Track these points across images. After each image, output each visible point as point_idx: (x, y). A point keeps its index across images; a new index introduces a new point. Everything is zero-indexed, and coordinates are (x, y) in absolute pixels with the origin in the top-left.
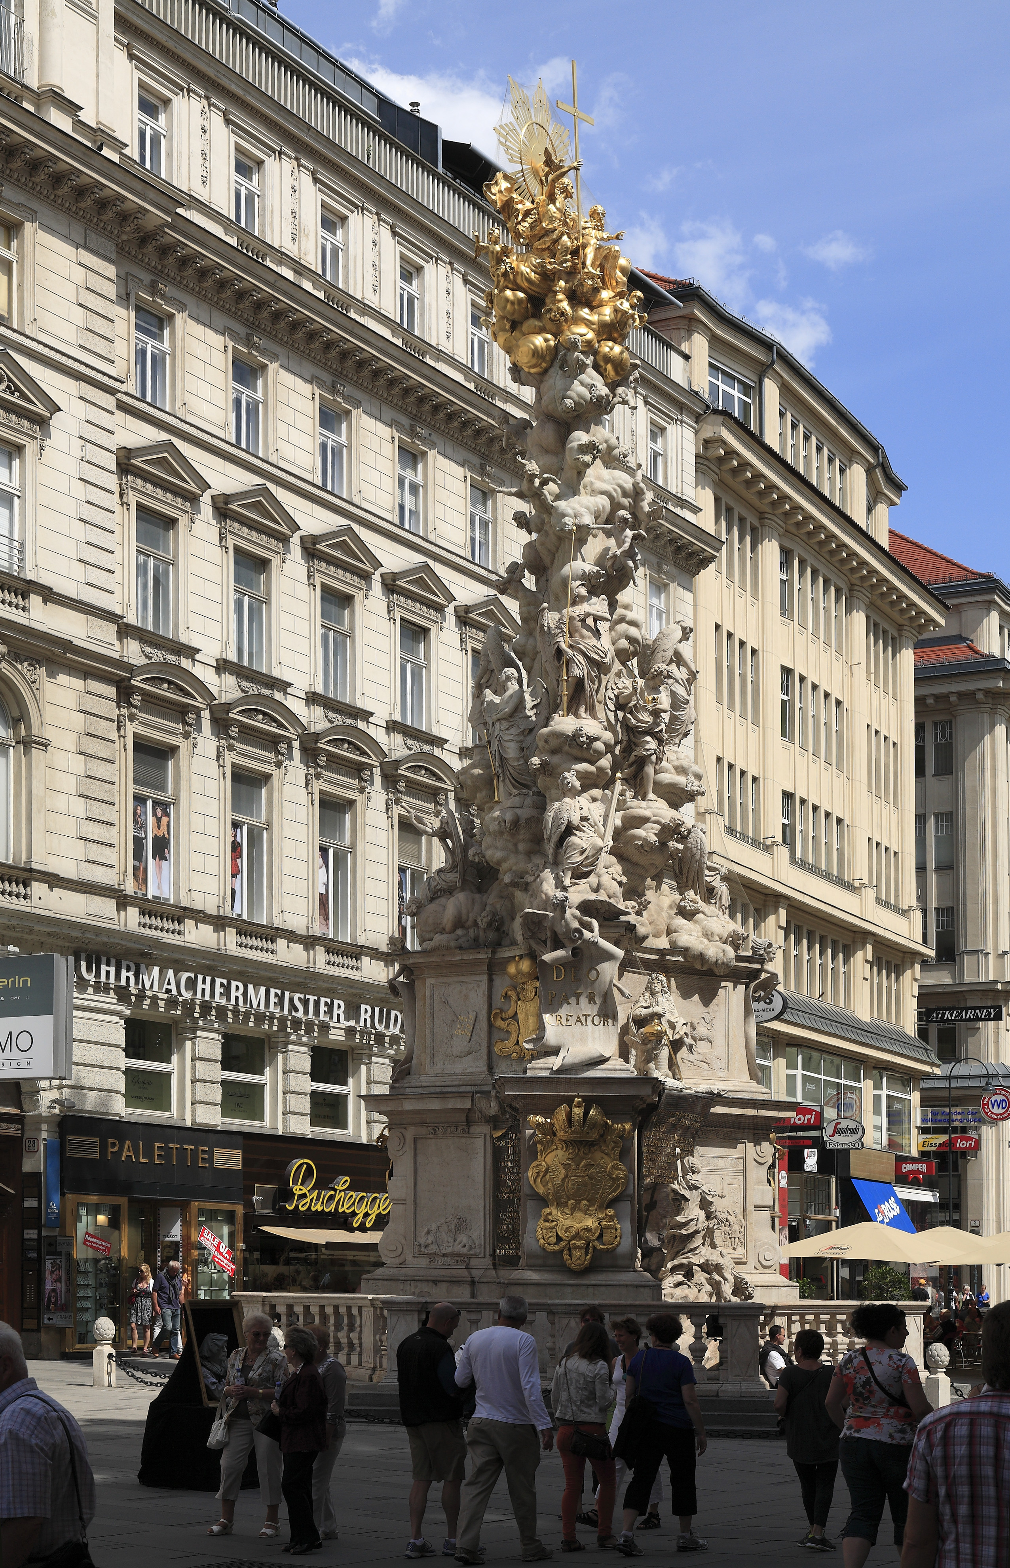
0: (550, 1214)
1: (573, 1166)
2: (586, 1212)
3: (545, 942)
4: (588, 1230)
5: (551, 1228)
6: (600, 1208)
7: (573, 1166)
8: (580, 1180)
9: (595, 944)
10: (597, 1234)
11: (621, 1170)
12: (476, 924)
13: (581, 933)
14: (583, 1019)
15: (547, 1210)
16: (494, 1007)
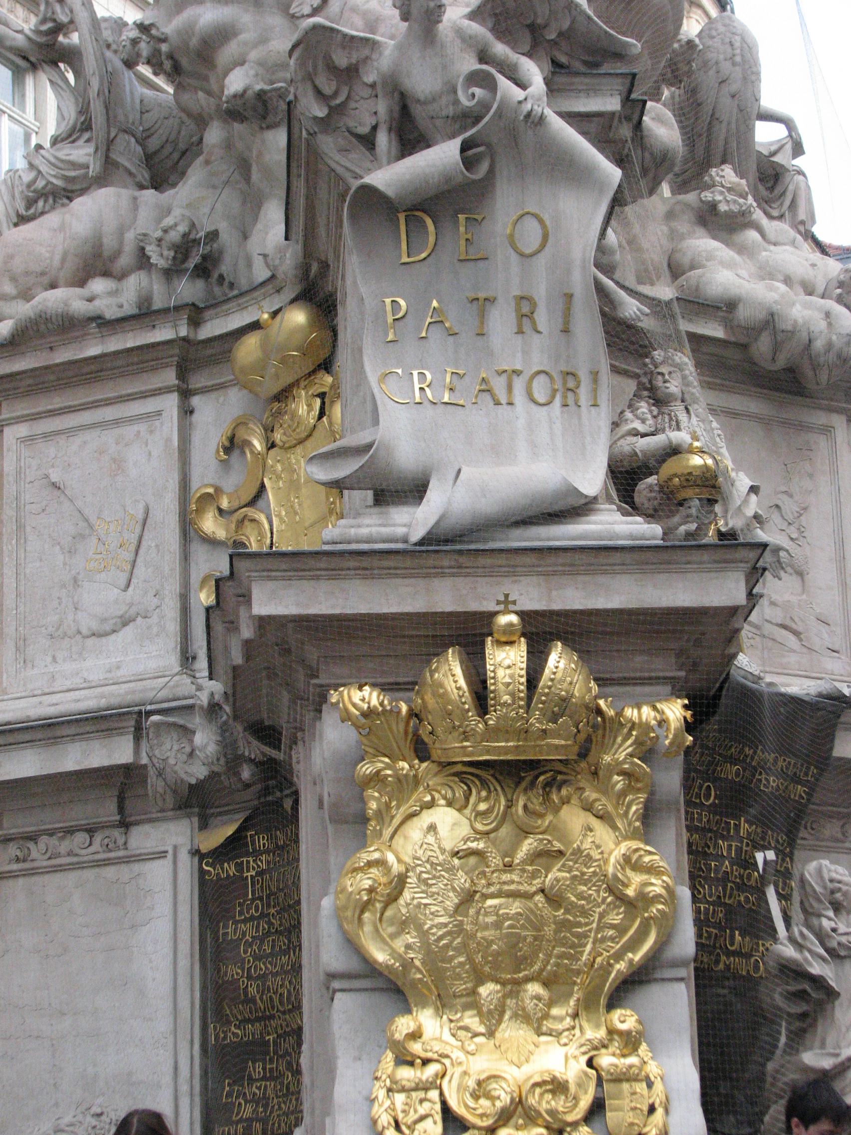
0: (415, 1035)
1: (495, 861)
2: (537, 1024)
3: (368, 141)
4: (557, 1086)
5: (425, 1087)
6: (587, 1006)
7: (495, 861)
8: (516, 907)
9: (536, 122)
10: (585, 1102)
11: (651, 870)
12: (143, 261)
13: (490, 84)
14: (499, 385)
15: (403, 1025)
16: (195, 483)
